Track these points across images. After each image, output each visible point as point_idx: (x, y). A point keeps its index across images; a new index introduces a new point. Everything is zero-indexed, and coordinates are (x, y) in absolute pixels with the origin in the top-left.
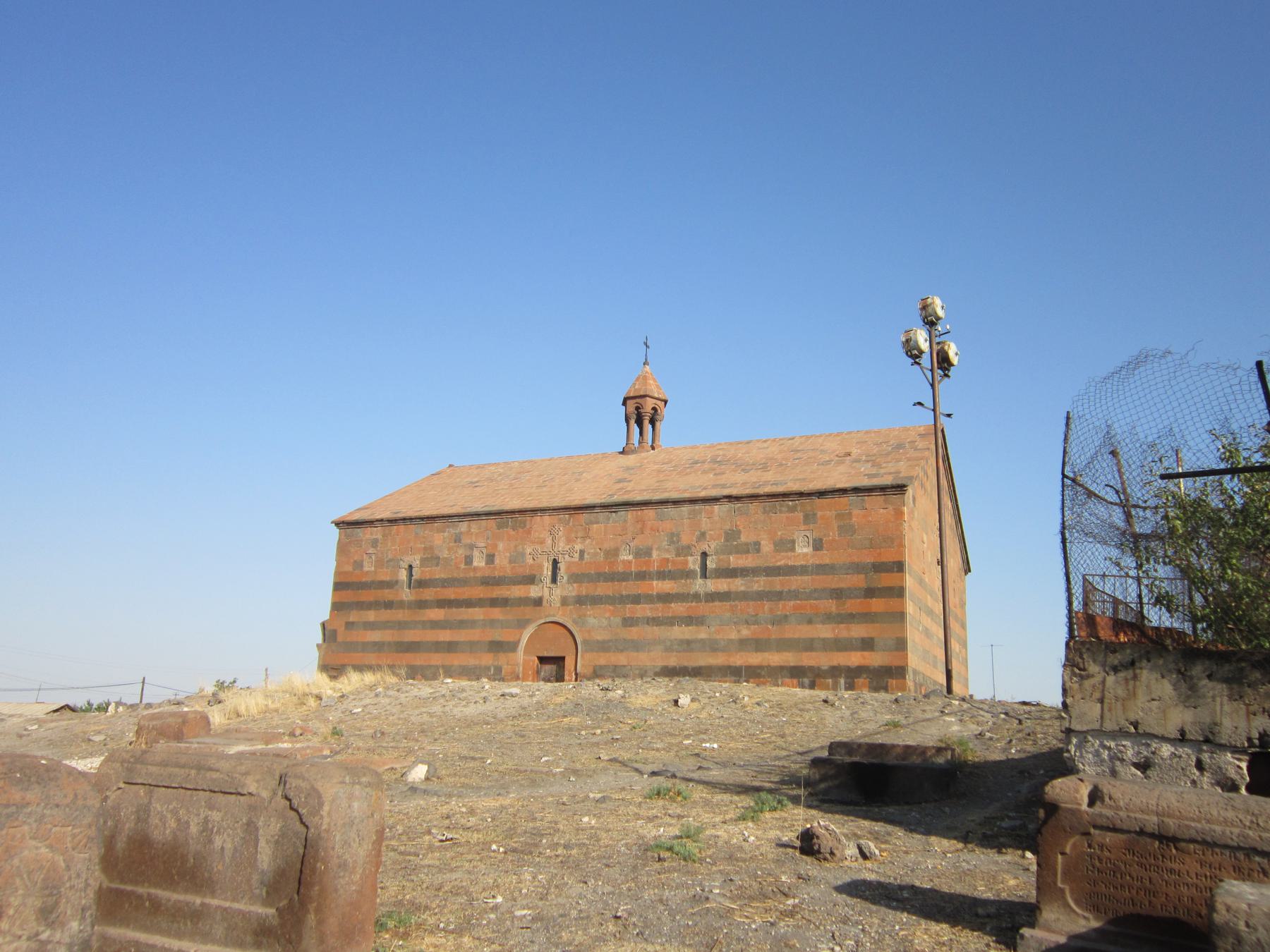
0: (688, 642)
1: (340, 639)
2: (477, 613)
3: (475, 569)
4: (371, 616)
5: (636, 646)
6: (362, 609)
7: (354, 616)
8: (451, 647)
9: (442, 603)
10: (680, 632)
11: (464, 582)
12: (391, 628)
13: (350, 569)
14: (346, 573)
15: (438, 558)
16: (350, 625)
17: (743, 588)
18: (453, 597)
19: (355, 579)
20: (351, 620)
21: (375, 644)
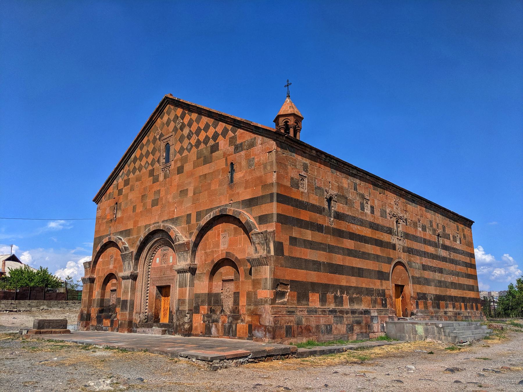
0: (440, 282)
1: (286, 253)
2: (370, 249)
3: (366, 214)
4: (309, 235)
5: (427, 282)
6: (301, 227)
7: (296, 233)
8: (359, 273)
9: (353, 236)
10: (437, 276)
11: (362, 223)
12: (324, 250)
13: (288, 184)
14: (285, 187)
15: (346, 198)
16: (293, 241)
17: (449, 257)
18: (357, 232)
19: (293, 196)
20: (294, 235)
21: (315, 262)
